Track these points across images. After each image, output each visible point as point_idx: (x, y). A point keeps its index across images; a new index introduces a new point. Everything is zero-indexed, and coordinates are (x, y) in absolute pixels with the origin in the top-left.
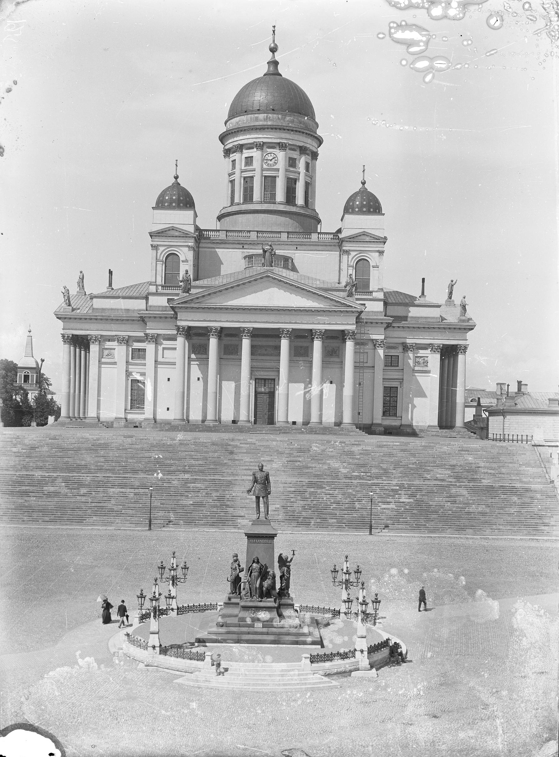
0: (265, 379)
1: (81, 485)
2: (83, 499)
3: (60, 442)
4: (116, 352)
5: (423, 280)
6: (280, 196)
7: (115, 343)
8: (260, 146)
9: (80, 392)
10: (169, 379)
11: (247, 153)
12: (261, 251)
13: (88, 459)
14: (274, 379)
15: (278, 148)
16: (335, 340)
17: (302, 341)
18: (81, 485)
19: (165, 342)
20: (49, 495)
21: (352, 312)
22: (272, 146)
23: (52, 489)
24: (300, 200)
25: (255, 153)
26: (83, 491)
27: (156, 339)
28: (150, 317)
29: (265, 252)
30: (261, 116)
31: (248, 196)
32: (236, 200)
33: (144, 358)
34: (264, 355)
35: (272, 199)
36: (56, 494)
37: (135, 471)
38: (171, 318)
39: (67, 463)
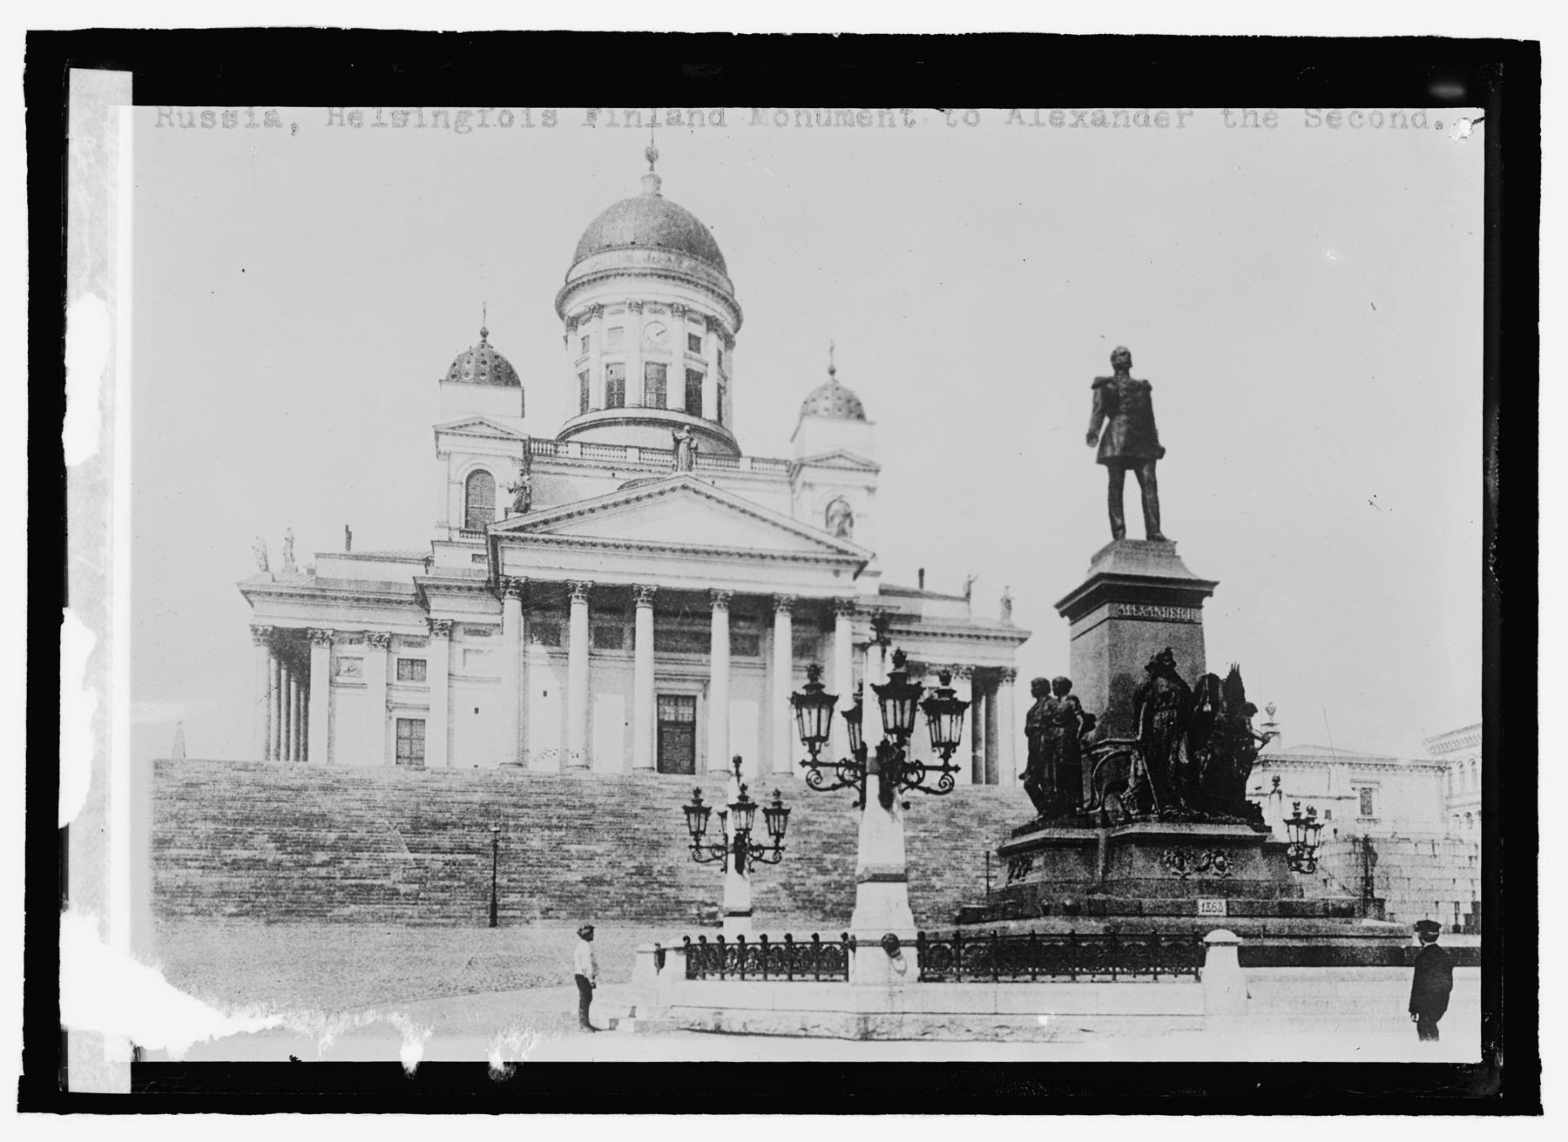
0: (677, 698)
1: (317, 846)
2: (323, 872)
3: (258, 776)
4: (363, 666)
5: (921, 573)
6: (676, 398)
7: (365, 646)
8: (639, 307)
9: (288, 732)
10: (477, 710)
11: (609, 320)
12: (670, 445)
13: (326, 803)
14: (694, 698)
15: (668, 312)
16: (817, 617)
17: (753, 613)
18: (317, 846)
19: (469, 638)
20: (235, 865)
21: (848, 562)
22: (657, 307)
23: (245, 854)
24: (709, 410)
25: (629, 319)
26: (320, 857)
27: (449, 629)
28: (437, 587)
29: (677, 442)
30: (639, 255)
31: (615, 395)
32: (591, 405)
33: (424, 679)
34: (672, 650)
35: (661, 403)
36: (254, 864)
37: (444, 826)
38: (481, 590)
39: (278, 811)
